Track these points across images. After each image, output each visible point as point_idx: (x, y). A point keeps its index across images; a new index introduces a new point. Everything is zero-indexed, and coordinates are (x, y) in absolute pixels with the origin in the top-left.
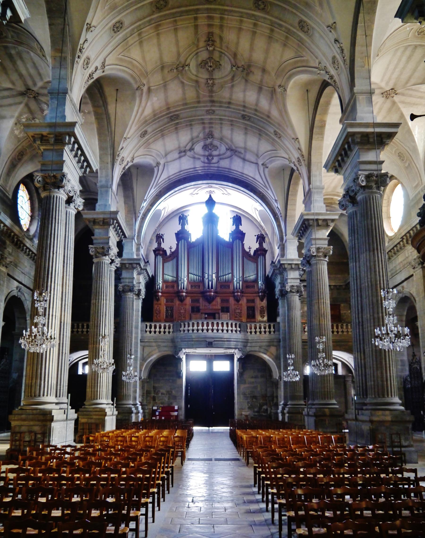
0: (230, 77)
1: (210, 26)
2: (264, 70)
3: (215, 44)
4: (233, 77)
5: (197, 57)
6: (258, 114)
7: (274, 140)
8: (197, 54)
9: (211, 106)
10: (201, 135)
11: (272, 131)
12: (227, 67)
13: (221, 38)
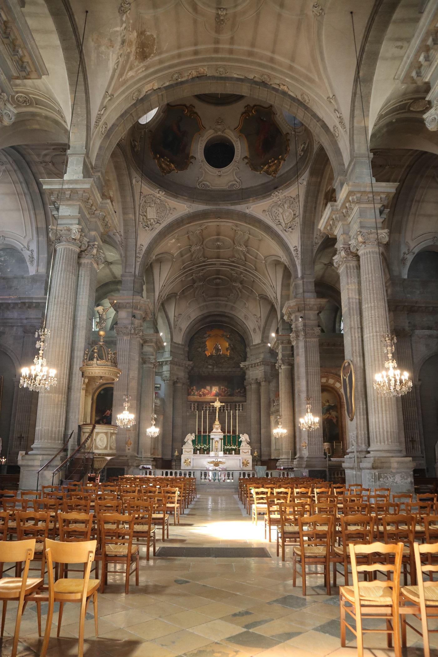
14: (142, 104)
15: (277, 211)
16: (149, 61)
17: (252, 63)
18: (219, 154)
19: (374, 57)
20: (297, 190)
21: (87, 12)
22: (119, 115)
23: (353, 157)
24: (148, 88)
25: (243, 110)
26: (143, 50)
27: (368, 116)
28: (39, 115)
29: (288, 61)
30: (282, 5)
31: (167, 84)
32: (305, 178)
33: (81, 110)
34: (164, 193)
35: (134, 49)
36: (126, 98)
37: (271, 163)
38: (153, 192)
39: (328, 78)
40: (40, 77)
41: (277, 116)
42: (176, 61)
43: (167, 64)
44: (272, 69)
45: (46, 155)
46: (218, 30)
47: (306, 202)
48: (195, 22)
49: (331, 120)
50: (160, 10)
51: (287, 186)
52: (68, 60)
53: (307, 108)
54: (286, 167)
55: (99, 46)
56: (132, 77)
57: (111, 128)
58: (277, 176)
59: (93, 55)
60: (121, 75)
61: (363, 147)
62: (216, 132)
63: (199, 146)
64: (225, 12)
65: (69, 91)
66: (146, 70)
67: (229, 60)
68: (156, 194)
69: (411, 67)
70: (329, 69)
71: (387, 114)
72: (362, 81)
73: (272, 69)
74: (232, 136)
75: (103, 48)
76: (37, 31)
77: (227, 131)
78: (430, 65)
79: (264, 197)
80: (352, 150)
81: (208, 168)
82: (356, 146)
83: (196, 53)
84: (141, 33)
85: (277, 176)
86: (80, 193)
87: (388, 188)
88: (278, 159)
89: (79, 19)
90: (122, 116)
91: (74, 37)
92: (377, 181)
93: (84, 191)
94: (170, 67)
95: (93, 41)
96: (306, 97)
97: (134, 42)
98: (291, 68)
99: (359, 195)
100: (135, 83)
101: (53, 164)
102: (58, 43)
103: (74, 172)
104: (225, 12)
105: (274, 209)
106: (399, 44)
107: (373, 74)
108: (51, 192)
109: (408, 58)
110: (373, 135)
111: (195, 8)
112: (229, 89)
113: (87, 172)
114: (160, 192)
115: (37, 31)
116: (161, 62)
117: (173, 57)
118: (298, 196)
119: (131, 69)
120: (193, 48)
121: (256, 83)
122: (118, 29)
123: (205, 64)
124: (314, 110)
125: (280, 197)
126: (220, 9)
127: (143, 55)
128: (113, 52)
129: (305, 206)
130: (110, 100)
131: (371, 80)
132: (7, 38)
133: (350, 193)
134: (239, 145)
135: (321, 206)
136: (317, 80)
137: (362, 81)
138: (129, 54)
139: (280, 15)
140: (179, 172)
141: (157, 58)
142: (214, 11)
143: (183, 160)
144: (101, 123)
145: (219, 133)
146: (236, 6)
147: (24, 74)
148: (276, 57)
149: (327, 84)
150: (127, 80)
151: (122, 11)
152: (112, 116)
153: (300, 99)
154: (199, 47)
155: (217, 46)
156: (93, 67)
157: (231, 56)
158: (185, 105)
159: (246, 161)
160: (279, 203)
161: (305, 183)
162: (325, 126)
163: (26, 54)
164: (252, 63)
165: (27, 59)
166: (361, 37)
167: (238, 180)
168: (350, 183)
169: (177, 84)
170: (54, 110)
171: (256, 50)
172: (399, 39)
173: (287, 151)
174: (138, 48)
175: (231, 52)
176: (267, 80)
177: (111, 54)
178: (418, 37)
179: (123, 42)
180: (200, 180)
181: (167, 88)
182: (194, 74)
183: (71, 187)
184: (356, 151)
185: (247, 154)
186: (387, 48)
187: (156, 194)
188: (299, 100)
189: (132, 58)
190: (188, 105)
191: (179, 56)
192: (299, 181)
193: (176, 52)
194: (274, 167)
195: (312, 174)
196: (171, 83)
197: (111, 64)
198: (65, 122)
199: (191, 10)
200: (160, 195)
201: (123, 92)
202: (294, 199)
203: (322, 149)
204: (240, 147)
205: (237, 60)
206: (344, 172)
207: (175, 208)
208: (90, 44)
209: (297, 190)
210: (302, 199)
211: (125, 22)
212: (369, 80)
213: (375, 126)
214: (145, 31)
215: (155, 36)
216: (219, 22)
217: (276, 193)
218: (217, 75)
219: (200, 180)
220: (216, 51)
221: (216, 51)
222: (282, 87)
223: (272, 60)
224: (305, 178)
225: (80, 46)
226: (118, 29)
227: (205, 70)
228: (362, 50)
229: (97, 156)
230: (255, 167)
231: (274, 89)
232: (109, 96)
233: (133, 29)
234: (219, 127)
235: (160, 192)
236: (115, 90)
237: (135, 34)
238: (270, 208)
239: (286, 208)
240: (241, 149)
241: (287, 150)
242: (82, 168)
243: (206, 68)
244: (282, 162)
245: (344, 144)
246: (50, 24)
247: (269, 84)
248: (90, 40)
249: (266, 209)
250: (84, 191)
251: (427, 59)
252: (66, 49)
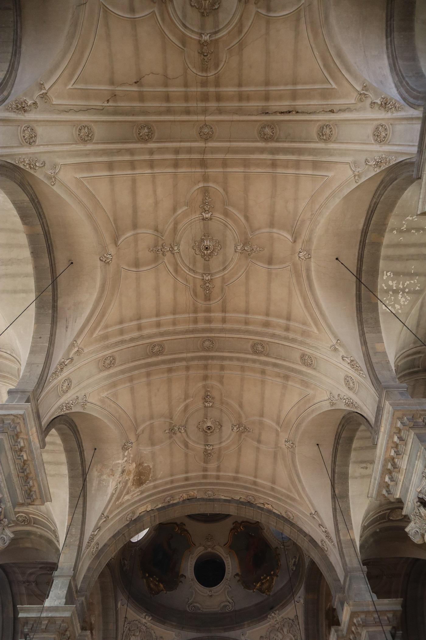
0: (180, 226)
1: (208, 310)
2: (137, 264)
3: (202, 283)
4: (175, 229)
5: (224, 262)
6: (128, 158)
7: (87, 110)
8: (224, 269)
9: (203, 151)
10: (224, 56)
11: (98, 132)
12: (185, 247)
13: (195, 294)
14: (135, 524)
15: (275, 637)
16: (144, 486)
17: (237, 486)
18: (210, 572)
19: (345, 477)
20: (294, 610)
21: (95, 449)
22: (112, 535)
23: (347, 572)
24: (142, 509)
25: (232, 526)
26: (140, 478)
27: (352, 528)
28: (35, 534)
29: (269, 484)
30: (259, 441)
31: (160, 506)
32: (300, 595)
33: (76, 531)
34: (150, 618)
35: (132, 477)
36: (120, 520)
37: (263, 580)
38: (138, 617)
39: (307, 496)
40: (43, 504)
41: (265, 531)
42: (168, 487)
43: (161, 489)
44: (256, 491)
45: (31, 574)
46: (206, 462)
47: (306, 623)
48: (186, 455)
49: (318, 535)
50: (157, 447)
51: (284, 606)
52: (71, 486)
53: (292, 525)
55: (102, 475)
56: (128, 500)
57: (102, 549)
58: (271, 594)
59: (95, 483)
60: (118, 498)
61: (354, 561)
62: (206, 548)
63: (189, 564)
64: (211, 448)
65: (67, 513)
66: (141, 494)
67: (217, 484)
68: (141, 619)
69: (380, 486)
70: (307, 489)
71: (369, 525)
72: (339, 498)
73: (256, 491)
74: (222, 552)
75: (105, 477)
76: (50, 463)
78: (396, 484)
80: (344, 564)
81: (198, 587)
82: (347, 559)
83: (187, 479)
84: (139, 465)
85: (271, 594)
86: (58, 622)
87: (391, 605)
88: (271, 575)
89: (88, 455)
90: (114, 536)
91: (81, 468)
92: (379, 597)
93: (64, 620)
94: (163, 491)
95: (97, 470)
96: (290, 514)
97: (133, 471)
98: (273, 489)
99: (363, 616)
100: (130, 506)
101: (37, 584)
102: (66, 472)
103: (56, 597)
104: (211, 448)
105: (272, 635)
106: (364, 465)
107: (347, 491)
108: (27, 620)
109: (375, 479)
110: (361, 546)
111: (186, 445)
112: (218, 509)
113: (70, 599)
114: (147, 617)
115: (50, 463)
116: (155, 487)
117: (166, 483)
118: (297, 616)
119: (128, 493)
120: (184, 475)
121: (242, 503)
122: (120, 461)
123: (195, 488)
124: (300, 526)
125: (277, 619)
126: (207, 445)
127: (139, 481)
128: (113, 480)
129: (306, 629)
130: (104, 521)
131: (347, 496)
132: (23, 472)
133: (353, 615)
134: (230, 560)
135: (324, 628)
136: (298, 498)
137: (339, 498)
138: (127, 480)
139: (258, 448)
140: (168, 592)
141: (152, 484)
142: (202, 447)
143: (173, 579)
144: (93, 544)
145: (210, 550)
146: (220, 443)
147: (29, 501)
148: (259, 480)
149: (308, 502)
150: (123, 503)
151: (124, 448)
152: (104, 536)
153: (285, 516)
154: (189, 475)
155: (205, 473)
156: (93, 492)
157: (218, 481)
158: (176, 523)
159: (238, 578)
160: (277, 626)
161: (302, 601)
162: (312, 541)
163: (36, 485)
164: (237, 486)
165: (35, 488)
166: (330, 462)
167: (231, 601)
168: (351, 603)
169: (169, 506)
170: (50, 529)
171: (240, 475)
172: (362, 462)
174: (135, 476)
175: (218, 477)
176: (252, 501)
177: (111, 481)
178: (379, 463)
179: (123, 472)
180: (190, 601)
181: (159, 510)
182: (185, 496)
183: (50, 615)
184: (349, 565)
185: (238, 571)
186: (353, 470)
187: (141, 619)
188: (283, 517)
189: (129, 484)
190: (179, 522)
191: (172, 482)
192: (296, 599)
193: (169, 479)
194: (267, 584)
195: (308, 590)
196: (163, 505)
197: (110, 490)
198: (58, 541)
199: (183, 447)
200: (146, 620)
201: (119, 513)
202: (293, 620)
203: (313, 563)
204: (230, 564)
205: (224, 484)
206: (342, 589)
207: (161, 637)
208: (94, 474)
209: (294, 610)
210: (301, 620)
211: (126, 456)
212: (345, 496)
213: (361, 537)
214: (143, 463)
215: (151, 467)
216: (207, 455)
217: (273, 614)
218: (205, 497)
219: (190, 601)
220: (205, 477)
221: (205, 477)
222: (266, 506)
223: (255, 483)
224: (300, 595)
225: (84, 475)
226: (120, 461)
227: (194, 493)
228: (333, 472)
229: (84, 578)
230: (247, 585)
231: (259, 507)
232: (105, 517)
233: (133, 462)
234: (209, 543)
235: (147, 617)
236: (111, 512)
237: (134, 465)
238: (268, 633)
239: (286, 633)
240: (231, 566)
242: (65, 592)
243: (196, 492)
244: (275, 578)
245: (334, 558)
246: (63, 458)
247: (255, 503)
248: (95, 469)
250: (63, 621)
251: (392, 479)
252: (72, 477)
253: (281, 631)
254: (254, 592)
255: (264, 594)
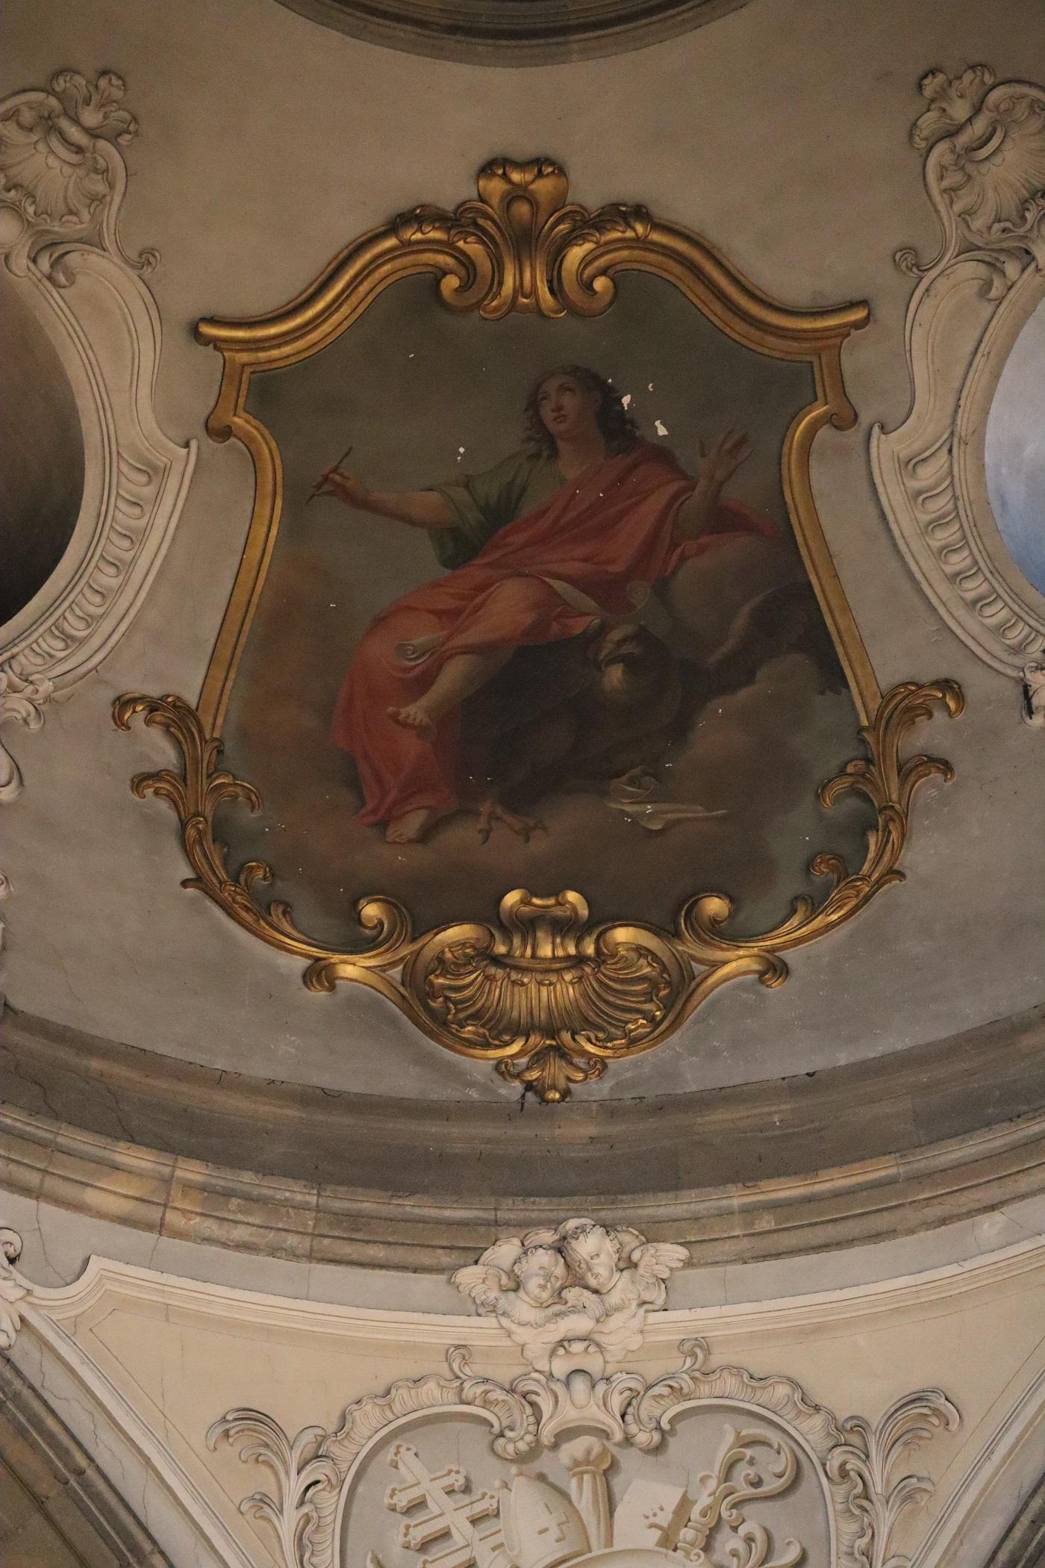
25: (450, 185)
37: (526, 926)
41: (886, 449)
54: (770, 1009)
77: (102, 272)
79: (354, 1223)
88: (672, 918)
105: (414, 1472)
118: (921, 1412)
125: (623, 1334)
160: (580, 1405)
173: (851, 857)
194: (565, 991)
202: (851, 1432)
204: (148, 557)
217: (593, 1247)
238: (369, 1423)
241: (846, 869)
249: (301, 1411)
253: (584, 1495)
254: (318, 974)
255: (480, 1063)
